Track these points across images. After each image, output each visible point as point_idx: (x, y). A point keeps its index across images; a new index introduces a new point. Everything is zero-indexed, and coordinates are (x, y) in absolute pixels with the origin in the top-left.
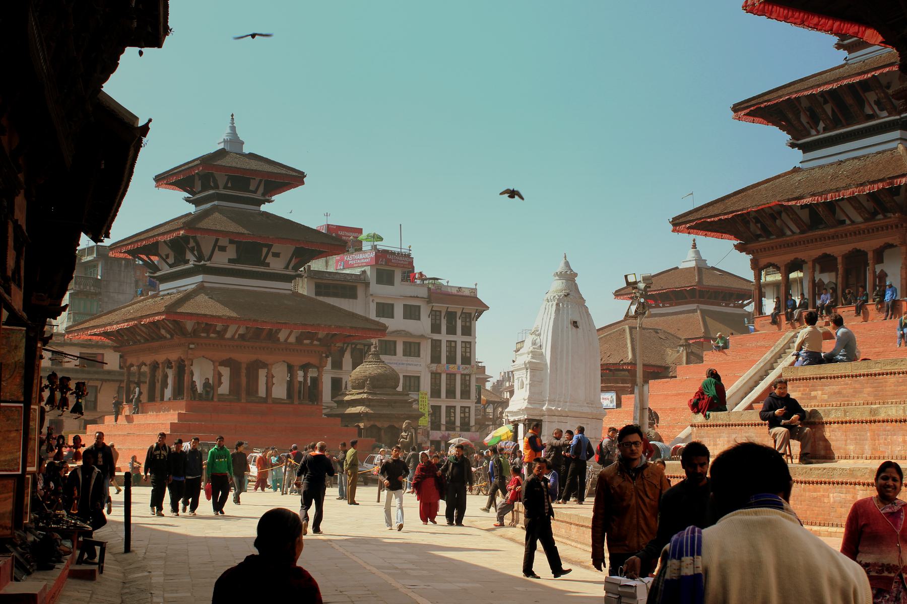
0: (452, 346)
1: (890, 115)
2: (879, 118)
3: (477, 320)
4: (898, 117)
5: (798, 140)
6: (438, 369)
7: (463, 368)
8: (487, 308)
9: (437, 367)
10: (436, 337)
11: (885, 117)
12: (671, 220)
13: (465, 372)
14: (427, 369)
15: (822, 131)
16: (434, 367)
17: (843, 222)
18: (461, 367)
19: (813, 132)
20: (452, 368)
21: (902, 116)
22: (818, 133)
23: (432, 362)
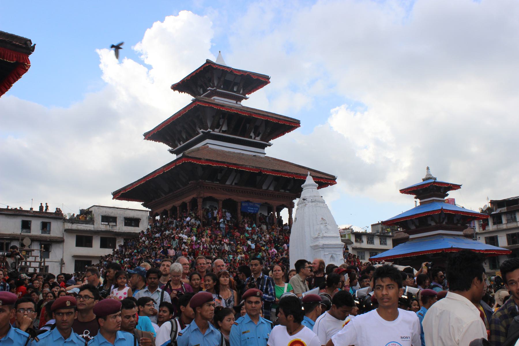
1: (261, 140)
2: (254, 139)
5: (210, 131)
22: (219, 132)
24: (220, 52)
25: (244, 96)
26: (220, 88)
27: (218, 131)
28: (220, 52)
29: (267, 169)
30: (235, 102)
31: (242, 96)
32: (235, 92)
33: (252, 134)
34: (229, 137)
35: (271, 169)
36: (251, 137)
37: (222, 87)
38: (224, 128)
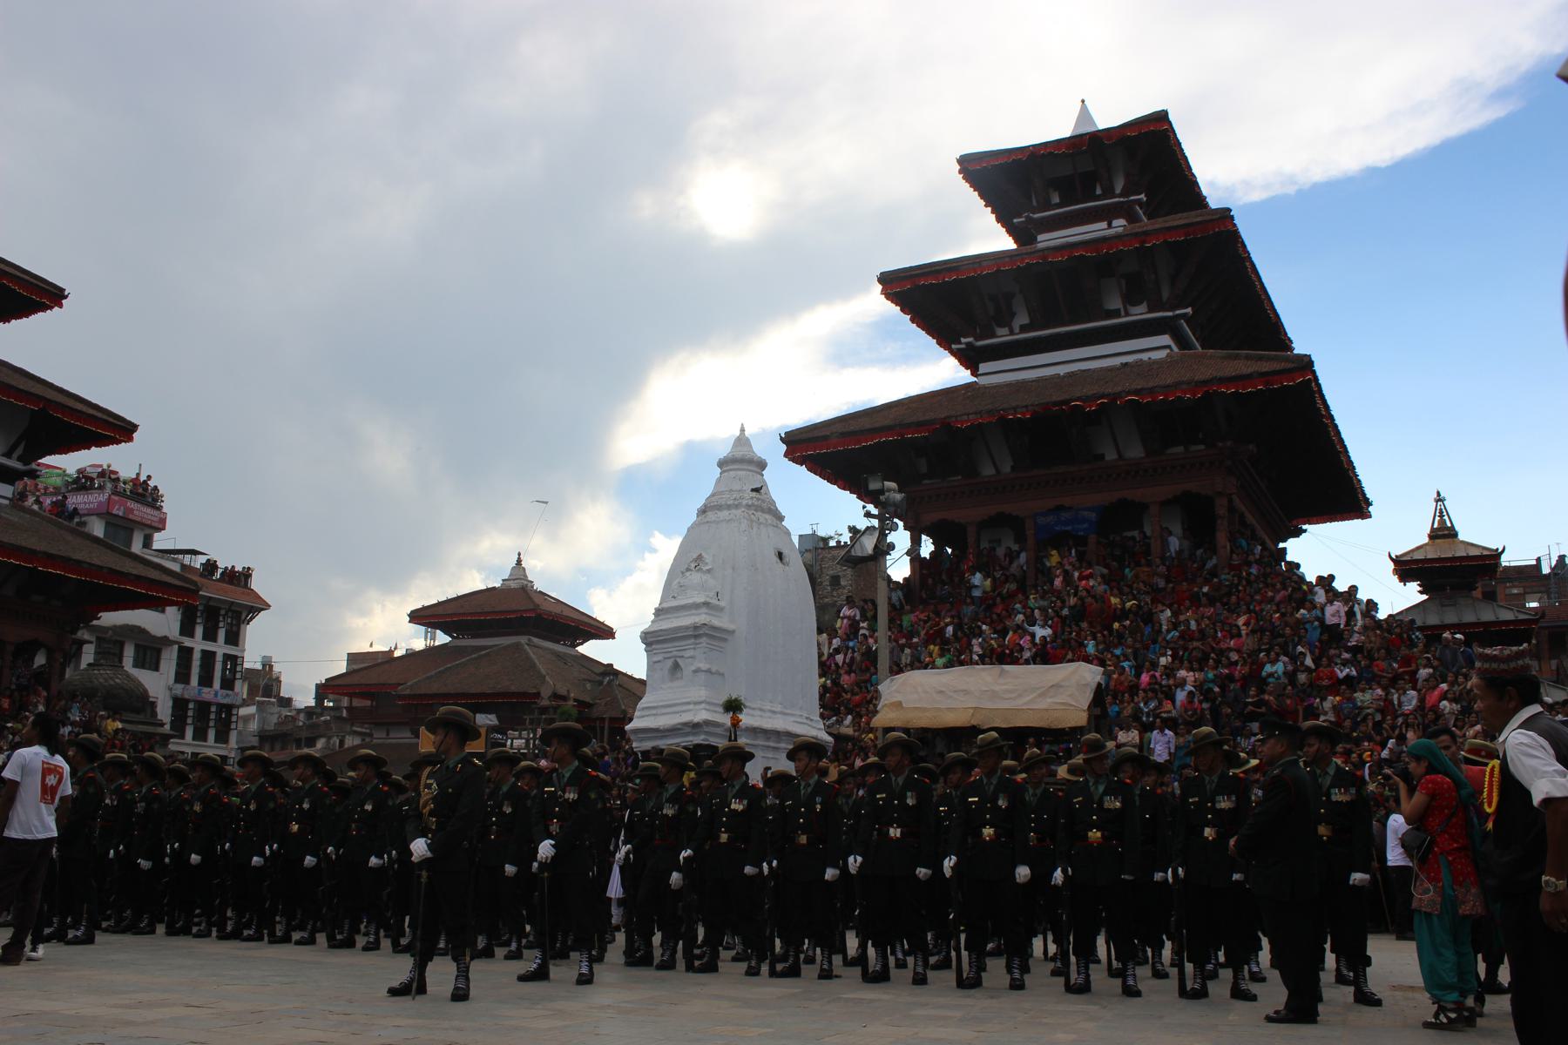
0: (208, 657)
1: (1150, 310)
2: (1127, 314)
3: (248, 624)
4: (1170, 314)
5: (977, 340)
6: (185, 692)
7: (222, 695)
8: (268, 606)
9: (183, 689)
10: (187, 642)
11: (1140, 313)
12: (783, 436)
13: (225, 701)
14: (168, 693)
15: (1017, 330)
16: (179, 689)
17: (1102, 457)
18: (219, 694)
19: (1005, 331)
20: (207, 694)
21: (1178, 312)
22: (1012, 333)
23: (177, 680)
24: (1083, 101)
25: (1122, 199)
26: (1049, 206)
27: (1008, 333)
28: (1083, 101)
29: (1026, 406)
30: (1104, 225)
31: (1117, 200)
32: (1098, 198)
33: (1115, 303)
34: (1039, 338)
35: (1036, 403)
36: (1116, 313)
37: (1056, 199)
38: (1022, 319)
